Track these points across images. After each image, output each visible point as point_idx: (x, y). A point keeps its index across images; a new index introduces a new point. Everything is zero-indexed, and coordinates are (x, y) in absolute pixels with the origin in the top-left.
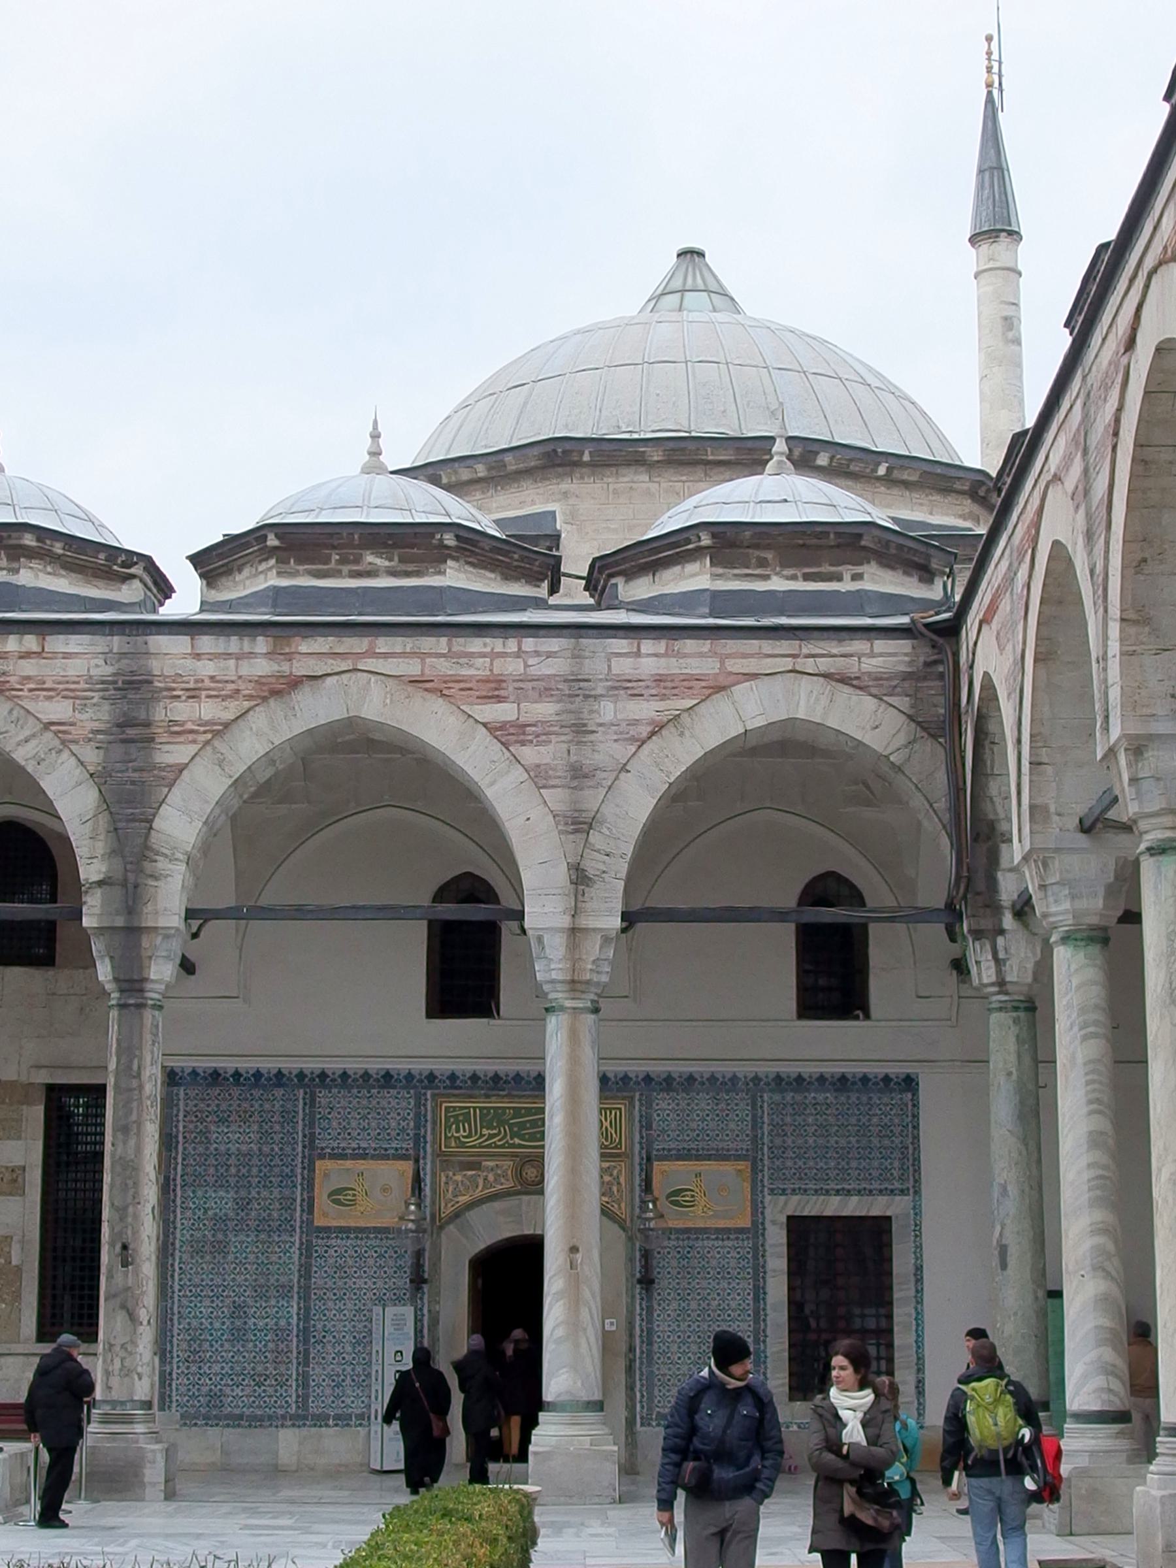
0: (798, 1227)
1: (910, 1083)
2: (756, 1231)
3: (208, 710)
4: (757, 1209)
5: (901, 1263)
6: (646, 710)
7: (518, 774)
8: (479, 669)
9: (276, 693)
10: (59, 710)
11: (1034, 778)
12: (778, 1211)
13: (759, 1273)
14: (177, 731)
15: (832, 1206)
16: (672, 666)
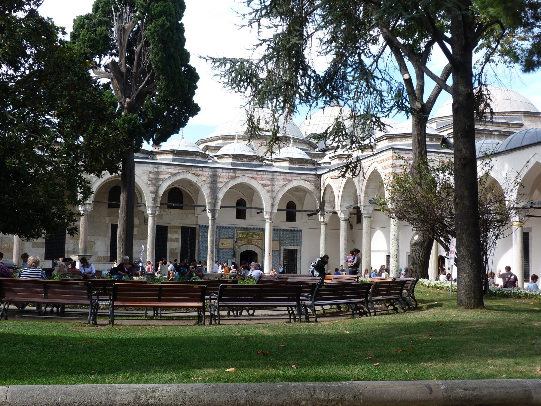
0: (285, 250)
1: (301, 231)
2: (280, 250)
3: (224, 180)
4: (280, 247)
5: (298, 256)
6: (281, 183)
7: (265, 191)
8: (260, 176)
9: (234, 178)
10: (205, 179)
11: (342, 204)
12: (282, 248)
13: (280, 256)
14: (221, 183)
15: (290, 247)
16: (285, 178)
